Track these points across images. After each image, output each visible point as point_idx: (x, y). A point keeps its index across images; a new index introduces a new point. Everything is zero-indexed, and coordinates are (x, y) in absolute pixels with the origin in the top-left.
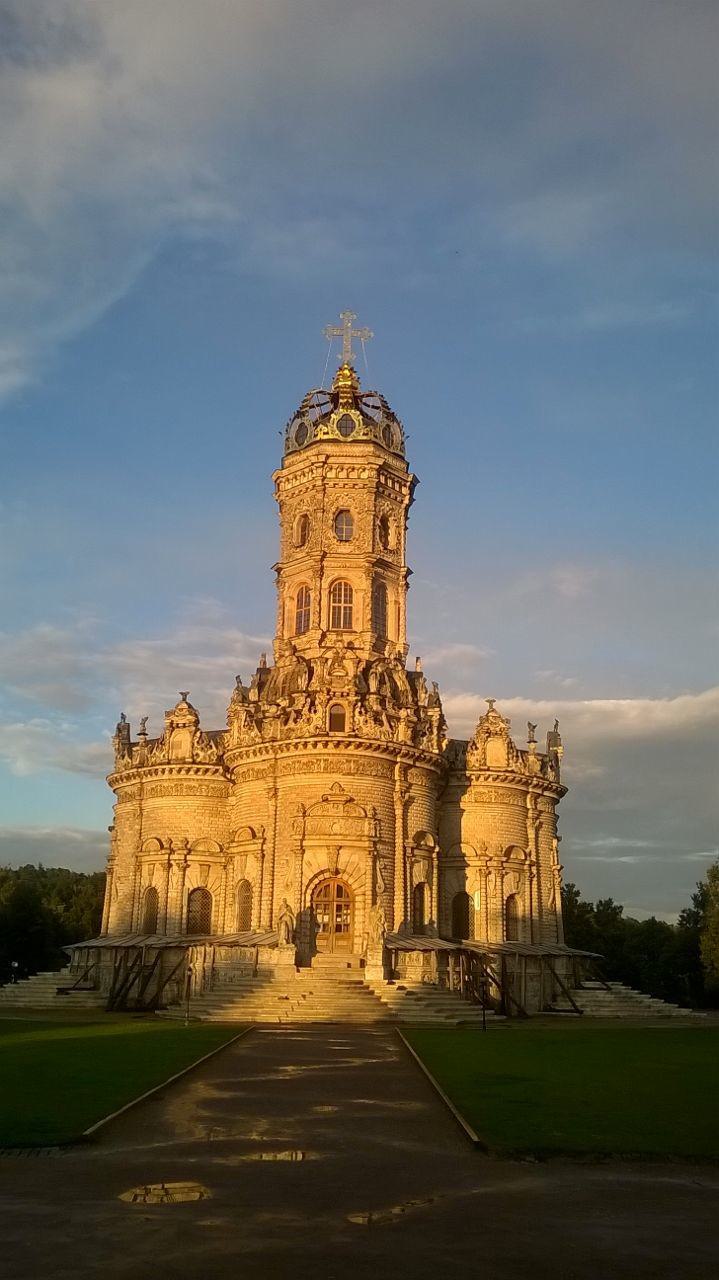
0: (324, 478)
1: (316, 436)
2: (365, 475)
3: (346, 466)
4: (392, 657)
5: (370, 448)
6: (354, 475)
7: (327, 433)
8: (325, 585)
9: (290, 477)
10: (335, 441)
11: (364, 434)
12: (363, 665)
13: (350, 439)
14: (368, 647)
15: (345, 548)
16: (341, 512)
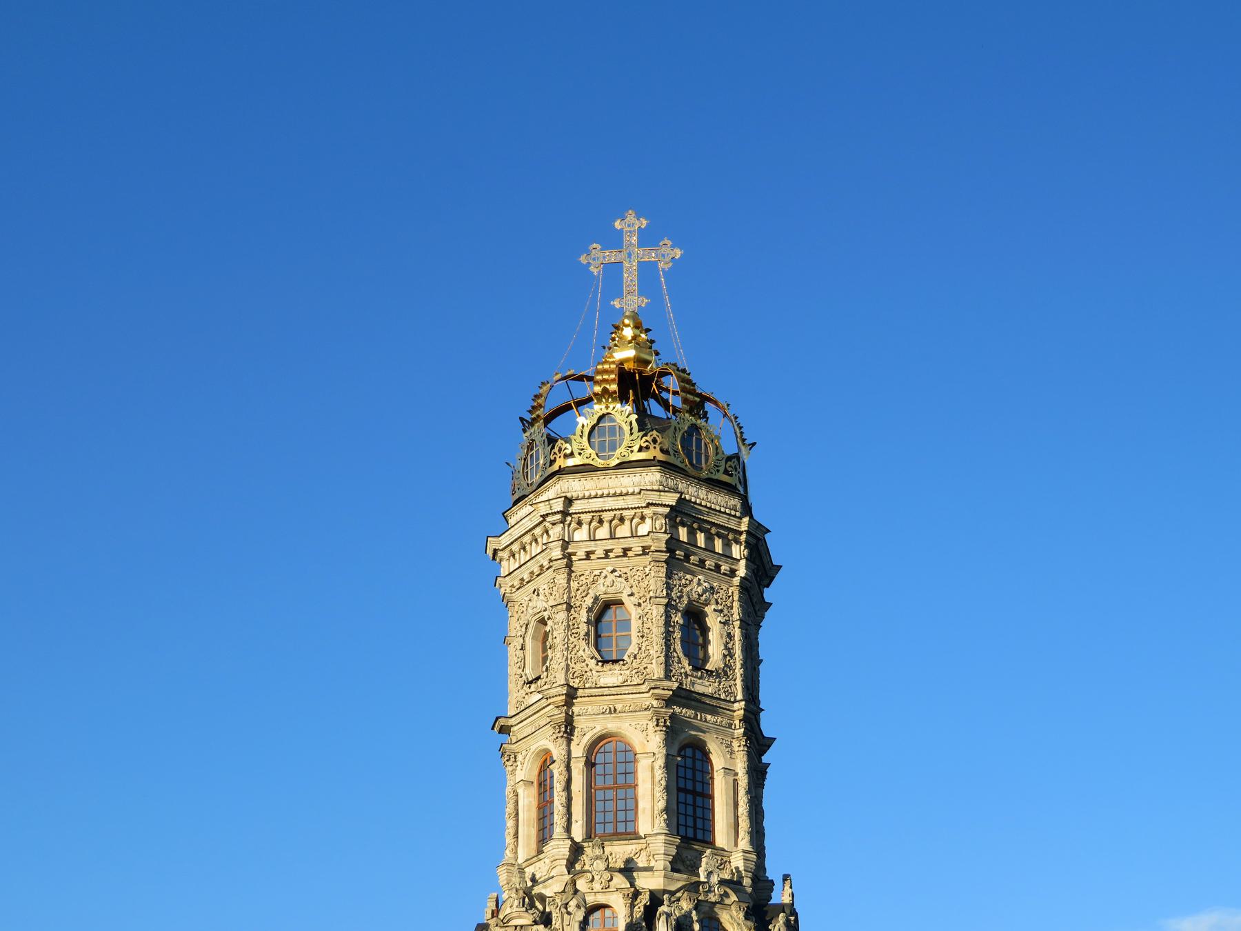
0: (565, 544)
1: (552, 462)
2: (644, 529)
3: (607, 516)
4: (714, 879)
5: (653, 477)
6: (623, 531)
7: (572, 454)
8: (578, 751)
9: (515, 547)
10: (585, 469)
11: (640, 450)
12: (644, 899)
13: (614, 462)
14: (661, 863)
15: (611, 676)
16: (607, 605)
